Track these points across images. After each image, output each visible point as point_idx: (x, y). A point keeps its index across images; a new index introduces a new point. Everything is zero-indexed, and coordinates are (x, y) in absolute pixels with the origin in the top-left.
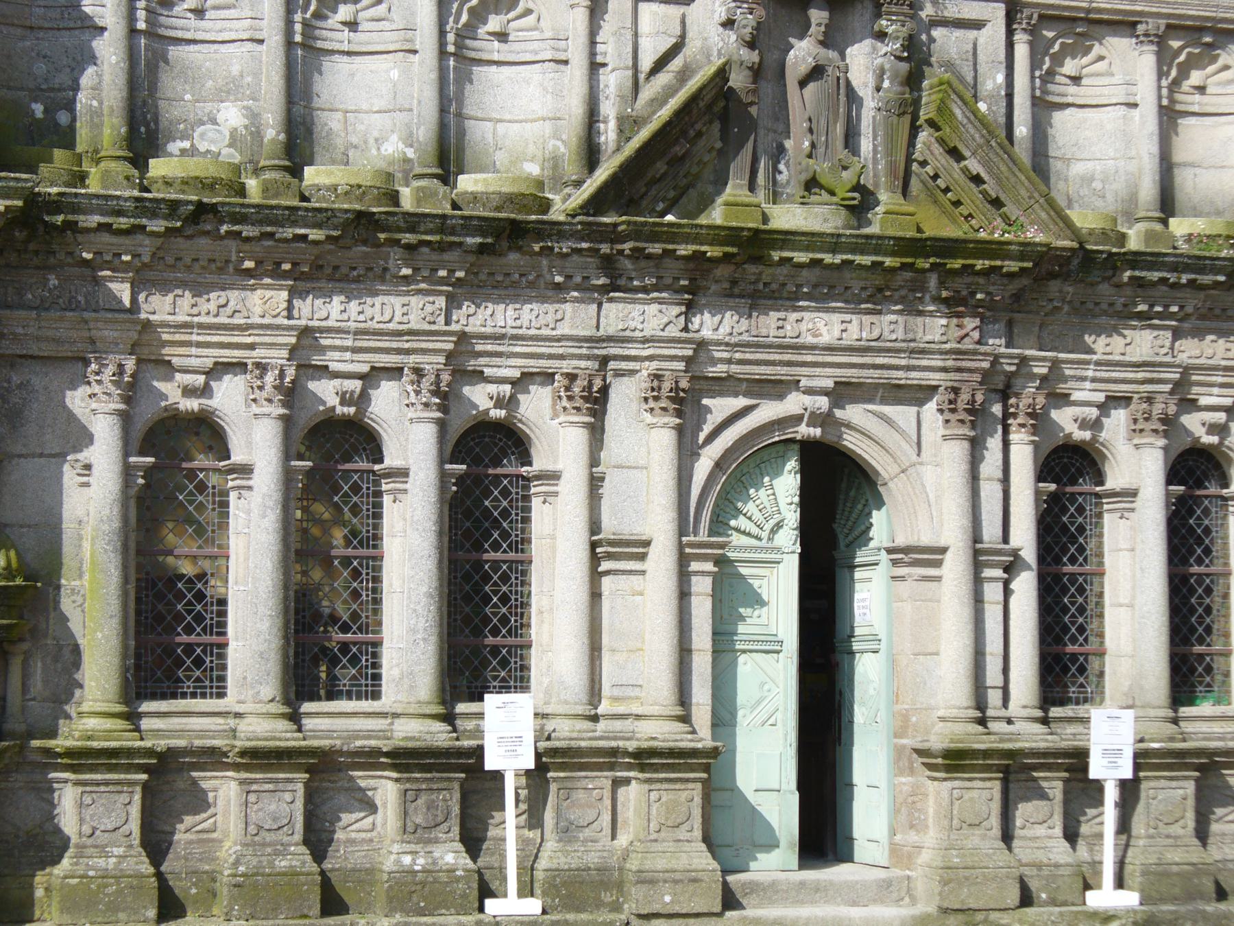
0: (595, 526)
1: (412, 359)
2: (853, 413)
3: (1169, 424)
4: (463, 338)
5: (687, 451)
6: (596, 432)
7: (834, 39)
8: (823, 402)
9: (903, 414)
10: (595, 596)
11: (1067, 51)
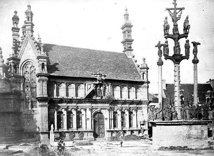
0: (86, 118)
1: (74, 108)
2: (102, 110)
3: (121, 110)
4: (78, 106)
5: (92, 113)
6: (86, 112)
7: (100, 87)
8: (100, 110)
9: (105, 110)
10: (86, 122)
11: (115, 87)
